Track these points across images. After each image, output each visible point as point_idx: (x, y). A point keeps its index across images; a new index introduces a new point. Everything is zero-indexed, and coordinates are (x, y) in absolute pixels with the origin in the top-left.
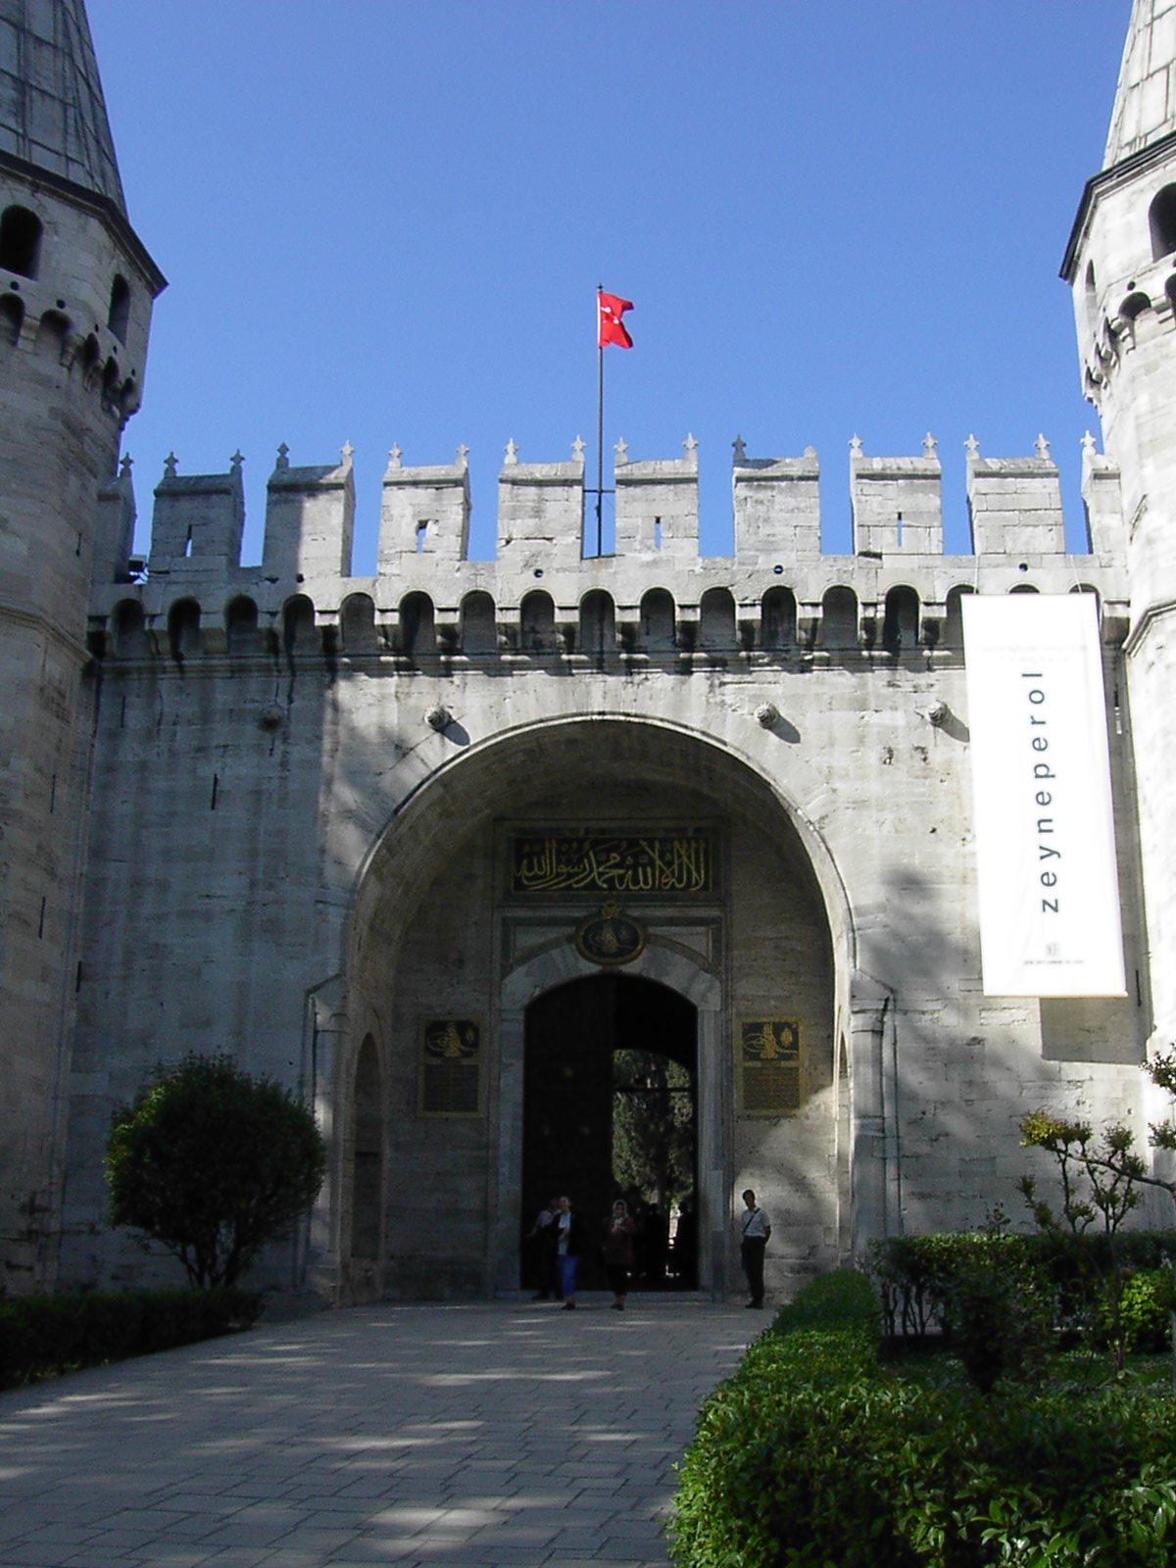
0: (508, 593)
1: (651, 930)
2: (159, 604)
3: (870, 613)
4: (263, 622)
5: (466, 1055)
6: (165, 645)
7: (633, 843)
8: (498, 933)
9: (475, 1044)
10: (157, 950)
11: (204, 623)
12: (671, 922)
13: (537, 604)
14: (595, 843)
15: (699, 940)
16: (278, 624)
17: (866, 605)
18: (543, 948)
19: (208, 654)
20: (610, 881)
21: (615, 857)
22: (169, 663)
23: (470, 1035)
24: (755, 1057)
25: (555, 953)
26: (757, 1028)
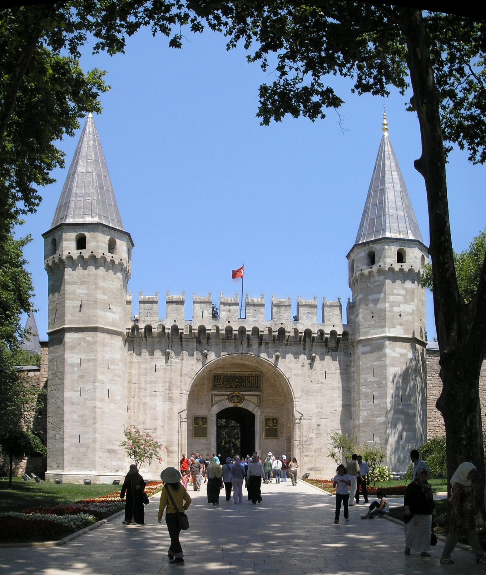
0: (223, 326)
1: (245, 397)
2: (142, 325)
3: (301, 335)
4: (167, 331)
5: (204, 424)
6: (143, 336)
7: (241, 377)
8: (210, 397)
9: (206, 422)
10: (145, 404)
11: (153, 330)
12: (250, 395)
13: (229, 330)
14: (232, 377)
15: (255, 400)
16: (170, 331)
17: (300, 333)
18: (220, 401)
19: (153, 337)
20: (236, 386)
21: (237, 380)
22: (144, 339)
23: (204, 420)
24: (268, 426)
25: (223, 402)
26: (269, 419)
